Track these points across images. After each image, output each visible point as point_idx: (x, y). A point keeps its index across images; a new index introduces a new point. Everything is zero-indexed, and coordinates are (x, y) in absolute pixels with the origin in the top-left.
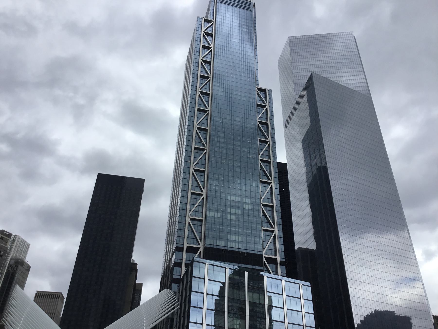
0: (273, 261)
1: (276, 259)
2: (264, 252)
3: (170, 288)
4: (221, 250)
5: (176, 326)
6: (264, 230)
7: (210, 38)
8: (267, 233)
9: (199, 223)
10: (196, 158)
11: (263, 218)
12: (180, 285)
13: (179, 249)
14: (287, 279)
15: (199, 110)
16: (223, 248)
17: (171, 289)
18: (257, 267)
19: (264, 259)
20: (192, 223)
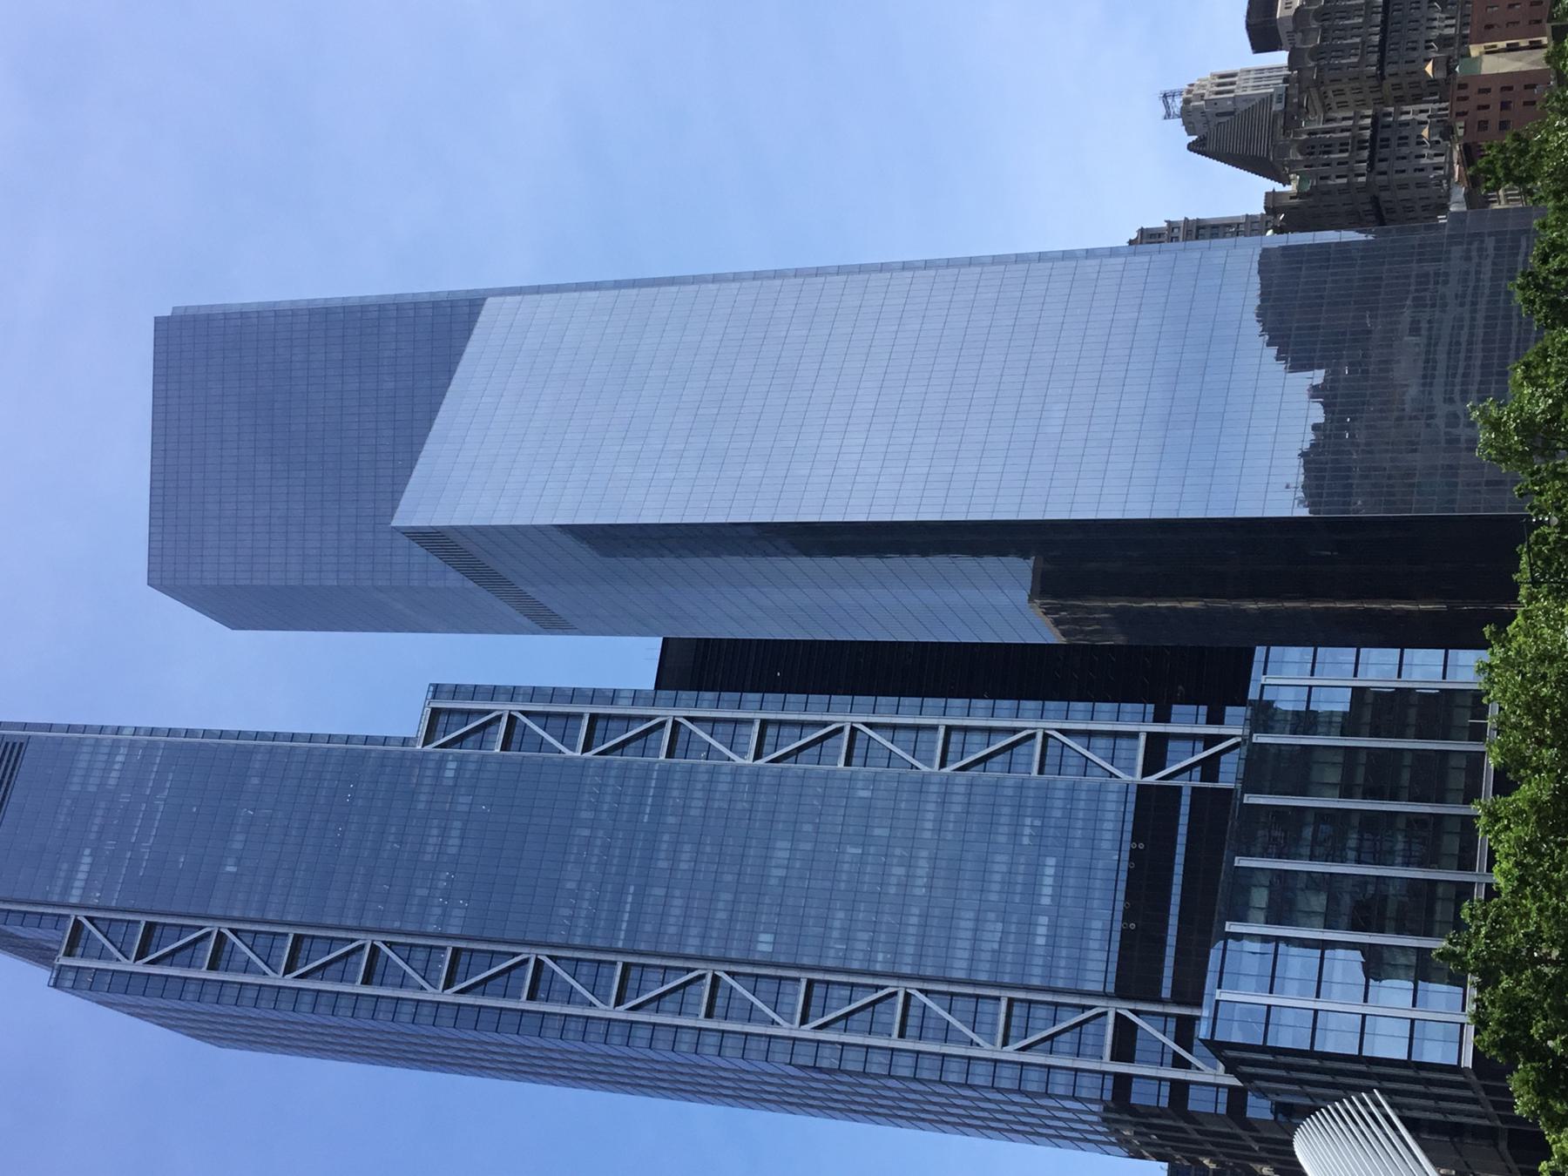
4: (1124, 933)
16: (1118, 926)
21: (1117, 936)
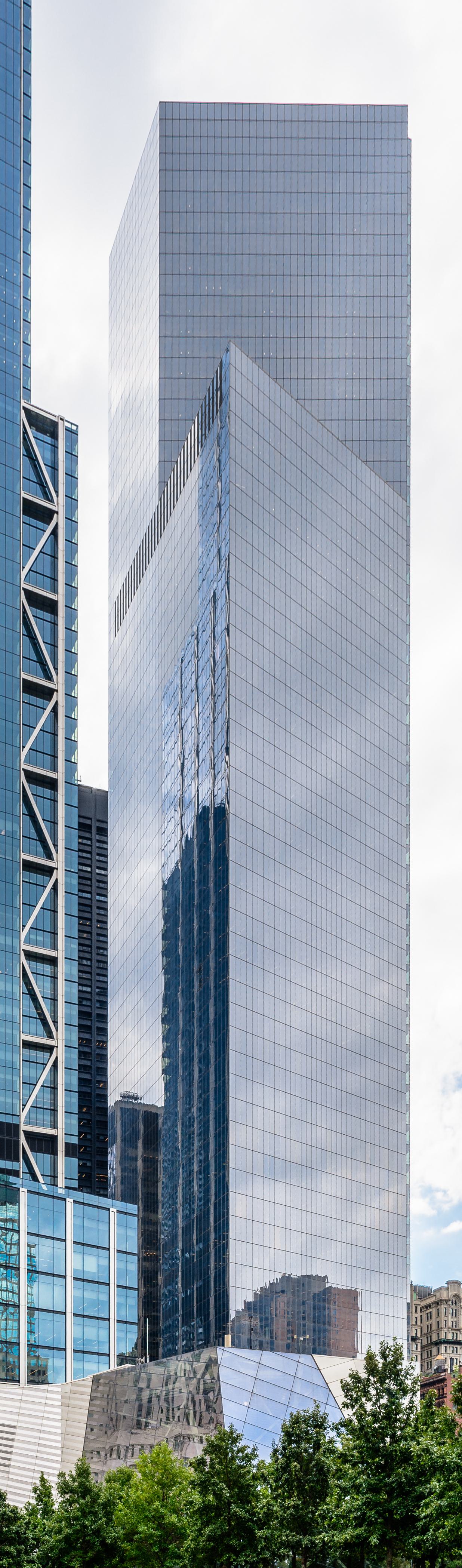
0: (44, 1144)
2: (23, 1115)
6: (27, 1045)
8: (33, 1053)
11: (26, 1004)
19: (23, 1140)
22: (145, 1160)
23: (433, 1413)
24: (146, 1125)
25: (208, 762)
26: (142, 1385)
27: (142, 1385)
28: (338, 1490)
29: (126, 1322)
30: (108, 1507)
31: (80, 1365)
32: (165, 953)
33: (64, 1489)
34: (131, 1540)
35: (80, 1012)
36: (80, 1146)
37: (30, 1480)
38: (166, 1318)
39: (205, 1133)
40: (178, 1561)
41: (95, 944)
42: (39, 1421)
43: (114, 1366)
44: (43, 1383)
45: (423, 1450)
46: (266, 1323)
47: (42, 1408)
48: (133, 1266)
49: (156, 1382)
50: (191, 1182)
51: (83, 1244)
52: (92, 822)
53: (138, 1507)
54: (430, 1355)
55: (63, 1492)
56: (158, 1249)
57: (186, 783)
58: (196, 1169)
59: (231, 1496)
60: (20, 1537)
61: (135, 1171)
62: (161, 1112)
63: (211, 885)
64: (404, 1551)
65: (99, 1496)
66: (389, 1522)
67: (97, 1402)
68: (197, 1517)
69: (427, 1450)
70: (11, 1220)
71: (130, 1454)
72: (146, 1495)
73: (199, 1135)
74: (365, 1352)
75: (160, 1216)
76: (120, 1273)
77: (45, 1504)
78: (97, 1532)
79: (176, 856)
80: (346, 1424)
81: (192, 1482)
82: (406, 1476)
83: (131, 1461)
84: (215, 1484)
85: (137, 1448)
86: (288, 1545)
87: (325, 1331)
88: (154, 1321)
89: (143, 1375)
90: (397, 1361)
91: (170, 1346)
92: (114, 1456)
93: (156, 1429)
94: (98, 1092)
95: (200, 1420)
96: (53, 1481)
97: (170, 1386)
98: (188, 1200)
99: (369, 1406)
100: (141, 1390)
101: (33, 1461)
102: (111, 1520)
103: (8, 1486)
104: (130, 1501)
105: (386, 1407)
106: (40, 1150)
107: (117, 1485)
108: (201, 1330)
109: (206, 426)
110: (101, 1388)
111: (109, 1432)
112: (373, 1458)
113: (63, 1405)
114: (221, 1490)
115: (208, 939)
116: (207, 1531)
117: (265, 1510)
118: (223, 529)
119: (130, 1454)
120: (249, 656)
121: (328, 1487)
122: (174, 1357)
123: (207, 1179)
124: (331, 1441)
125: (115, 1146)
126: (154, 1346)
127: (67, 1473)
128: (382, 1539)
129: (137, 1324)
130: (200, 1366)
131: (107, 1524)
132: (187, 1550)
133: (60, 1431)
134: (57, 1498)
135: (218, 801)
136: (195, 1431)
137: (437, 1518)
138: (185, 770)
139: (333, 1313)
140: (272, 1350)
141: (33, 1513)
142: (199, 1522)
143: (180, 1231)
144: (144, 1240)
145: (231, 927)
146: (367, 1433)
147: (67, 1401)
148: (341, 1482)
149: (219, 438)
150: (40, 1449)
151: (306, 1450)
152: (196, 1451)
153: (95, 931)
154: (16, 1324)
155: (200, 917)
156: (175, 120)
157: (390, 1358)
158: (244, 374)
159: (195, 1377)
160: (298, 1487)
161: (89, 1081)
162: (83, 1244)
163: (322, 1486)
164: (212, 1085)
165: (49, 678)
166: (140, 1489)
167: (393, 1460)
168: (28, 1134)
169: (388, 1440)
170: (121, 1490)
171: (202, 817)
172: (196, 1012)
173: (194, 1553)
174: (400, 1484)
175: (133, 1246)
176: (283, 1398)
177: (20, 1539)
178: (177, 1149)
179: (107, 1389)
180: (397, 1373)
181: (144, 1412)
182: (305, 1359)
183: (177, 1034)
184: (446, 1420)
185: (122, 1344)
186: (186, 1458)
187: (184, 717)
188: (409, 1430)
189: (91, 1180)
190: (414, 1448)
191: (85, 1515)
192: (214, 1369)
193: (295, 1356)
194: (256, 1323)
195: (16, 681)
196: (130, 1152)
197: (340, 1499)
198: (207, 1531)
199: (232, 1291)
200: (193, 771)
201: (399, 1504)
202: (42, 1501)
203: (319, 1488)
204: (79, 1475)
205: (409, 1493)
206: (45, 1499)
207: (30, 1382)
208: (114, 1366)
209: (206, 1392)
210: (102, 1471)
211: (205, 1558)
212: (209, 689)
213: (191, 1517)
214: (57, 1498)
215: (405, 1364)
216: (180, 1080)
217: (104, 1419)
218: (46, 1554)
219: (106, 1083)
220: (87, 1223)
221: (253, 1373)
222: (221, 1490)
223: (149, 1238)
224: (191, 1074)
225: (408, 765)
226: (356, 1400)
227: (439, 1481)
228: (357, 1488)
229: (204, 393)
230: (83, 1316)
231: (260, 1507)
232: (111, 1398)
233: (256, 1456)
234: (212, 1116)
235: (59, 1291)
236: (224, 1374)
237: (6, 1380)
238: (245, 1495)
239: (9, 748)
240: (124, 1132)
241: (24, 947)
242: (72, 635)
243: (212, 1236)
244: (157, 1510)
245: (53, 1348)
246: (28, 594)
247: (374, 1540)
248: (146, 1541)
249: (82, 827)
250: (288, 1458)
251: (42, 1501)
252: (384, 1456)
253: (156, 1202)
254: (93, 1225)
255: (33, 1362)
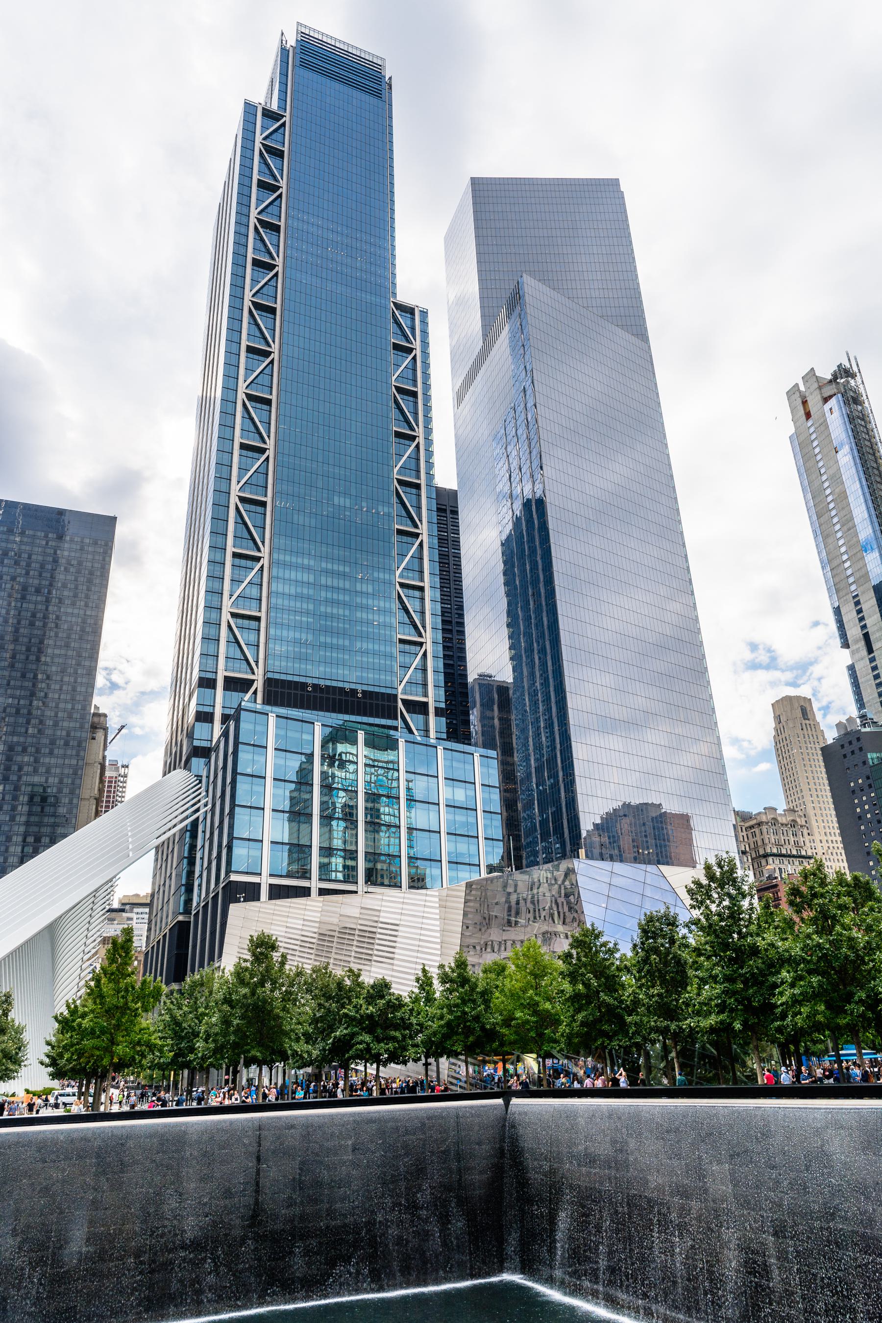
0: (420, 708)
1: (427, 703)
3: (187, 766)
4: (304, 685)
5: (203, 846)
6: (402, 641)
7: (278, 160)
8: (407, 647)
9: (254, 624)
10: (243, 470)
11: (401, 616)
12: (209, 761)
13: (207, 683)
14: (449, 745)
15: (250, 349)
16: (309, 681)
17: (190, 770)
18: (383, 722)
19: (400, 705)
20: (236, 624)
21: (303, 680)
22: (500, 719)
23: (772, 913)
24: (499, 696)
25: (528, 474)
26: (510, 889)
27: (510, 889)
28: (697, 980)
29: (493, 839)
30: (486, 995)
31: (454, 874)
32: (506, 584)
33: (445, 979)
34: (509, 1026)
35: (443, 621)
36: (447, 710)
37: (413, 971)
38: (527, 837)
39: (547, 700)
40: (555, 1045)
41: (452, 578)
42: (420, 920)
43: (484, 874)
44: (422, 888)
45: (769, 945)
46: (614, 840)
47: (422, 909)
48: (496, 796)
49: (522, 887)
50: (539, 734)
51: (453, 780)
52: (447, 507)
53: (513, 995)
54: (760, 865)
55: (443, 982)
56: (515, 783)
57: (513, 486)
58: (542, 725)
59: (599, 986)
60: (404, 1023)
61: (493, 726)
62: (511, 686)
63: (537, 543)
64: (767, 1036)
65: (477, 986)
66: (749, 1009)
67: (471, 904)
68: (569, 1004)
69: (772, 945)
70: (392, 762)
71: (503, 948)
72: (520, 985)
73: (543, 701)
74: (703, 862)
75: (516, 759)
76: (484, 801)
77: (428, 993)
78: (477, 1018)
79: (510, 526)
80: (696, 922)
81: (562, 973)
82: (757, 968)
83: (504, 954)
84: (583, 975)
85: (509, 943)
86: (657, 1030)
87: (665, 846)
88: (517, 838)
89: (510, 882)
90: (732, 870)
91: (532, 858)
92: (489, 950)
93: (526, 926)
94: (459, 672)
95: (564, 919)
96: (434, 972)
97: (535, 891)
98: (538, 747)
99: (713, 908)
100: (509, 894)
101: (415, 954)
102: (489, 1007)
103: (392, 976)
104: (506, 990)
105: (729, 908)
106: (415, 713)
107: (493, 976)
108: (558, 845)
109: (511, 309)
110: (473, 892)
111: (483, 930)
112: (725, 952)
113: (440, 906)
114: (589, 980)
115: (538, 576)
116: (580, 1017)
117: (632, 997)
118: (527, 357)
119: (503, 948)
120: (550, 420)
121: (687, 977)
122: (536, 867)
123: (552, 733)
124: (684, 937)
125: (475, 710)
126: (518, 858)
127: (447, 964)
128: (745, 1024)
129: (502, 841)
130: (560, 874)
131: (486, 1010)
132: (562, 1035)
133: (438, 929)
134: (438, 987)
135: (538, 495)
136: (560, 928)
137: (793, 1005)
138: (512, 479)
139: (670, 832)
140: (621, 861)
141: (416, 1000)
142: (571, 1009)
143: (533, 770)
144: (504, 777)
145: (555, 568)
146: (715, 930)
147: (444, 903)
148: (699, 973)
149: (520, 315)
150: (421, 943)
151: (662, 945)
152: (563, 945)
153: (452, 570)
154: (397, 841)
155: (531, 562)
156: (479, 186)
157: (726, 868)
158: (531, 287)
159: (556, 883)
160: (660, 977)
161: (452, 665)
162: (453, 780)
163: (682, 977)
164: (550, 668)
165: (414, 430)
166: (514, 980)
167: (743, 953)
168: (404, 701)
169: (735, 936)
170: (497, 980)
171: (527, 504)
172: (533, 621)
173: (570, 1037)
174: (753, 974)
175: (495, 780)
176: (637, 900)
177: (404, 1025)
178: (526, 711)
179: (479, 893)
180: (734, 880)
181: (513, 912)
182: (651, 868)
183: (519, 635)
184: (785, 919)
185: (490, 857)
186: (554, 952)
187: (509, 450)
188: (753, 928)
189: (457, 732)
190: (760, 943)
191: (464, 1002)
192: (572, 876)
193: (643, 866)
194: (605, 840)
195: (390, 432)
196: (488, 714)
197: (699, 988)
198: (580, 1017)
199: (582, 816)
200: (518, 479)
201: (755, 993)
202: (424, 990)
203: (679, 978)
204: (457, 966)
205: (764, 981)
206: (427, 988)
207: (411, 887)
208: (484, 874)
209: (567, 896)
210: (479, 964)
211: (579, 1042)
212: (525, 436)
213: (563, 1004)
214: (438, 987)
215: (739, 873)
216: (524, 664)
217: (478, 918)
218: (430, 1039)
219: (465, 666)
220: (455, 764)
221: (607, 880)
222: (589, 980)
223: (508, 775)
224: (533, 660)
225: (672, 476)
226: (702, 902)
227: (788, 972)
228: (714, 978)
229: (508, 295)
230: (455, 834)
231: (626, 995)
232: (483, 900)
233: (618, 950)
234: (552, 689)
235: (433, 815)
236: (581, 881)
237: (389, 886)
238: (611, 984)
239: (385, 467)
240: (482, 699)
241: (398, 580)
242: (428, 408)
243: (561, 774)
244: (531, 998)
245: (431, 860)
246: (397, 388)
247: (738, 1026)
248: (523, 1026)
249: (439, 510)
250: (647, 951)
251: (424, 990)
252: (734, 950)
253: (512, 749)
254: (461, 765)
255: (413, 871)
